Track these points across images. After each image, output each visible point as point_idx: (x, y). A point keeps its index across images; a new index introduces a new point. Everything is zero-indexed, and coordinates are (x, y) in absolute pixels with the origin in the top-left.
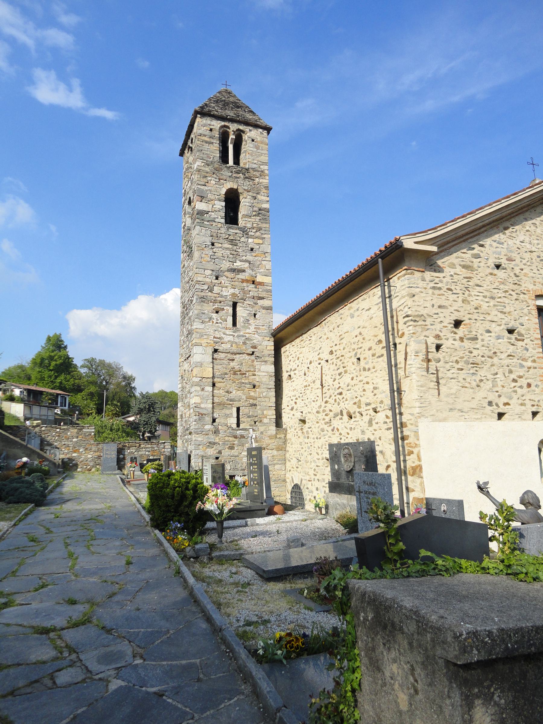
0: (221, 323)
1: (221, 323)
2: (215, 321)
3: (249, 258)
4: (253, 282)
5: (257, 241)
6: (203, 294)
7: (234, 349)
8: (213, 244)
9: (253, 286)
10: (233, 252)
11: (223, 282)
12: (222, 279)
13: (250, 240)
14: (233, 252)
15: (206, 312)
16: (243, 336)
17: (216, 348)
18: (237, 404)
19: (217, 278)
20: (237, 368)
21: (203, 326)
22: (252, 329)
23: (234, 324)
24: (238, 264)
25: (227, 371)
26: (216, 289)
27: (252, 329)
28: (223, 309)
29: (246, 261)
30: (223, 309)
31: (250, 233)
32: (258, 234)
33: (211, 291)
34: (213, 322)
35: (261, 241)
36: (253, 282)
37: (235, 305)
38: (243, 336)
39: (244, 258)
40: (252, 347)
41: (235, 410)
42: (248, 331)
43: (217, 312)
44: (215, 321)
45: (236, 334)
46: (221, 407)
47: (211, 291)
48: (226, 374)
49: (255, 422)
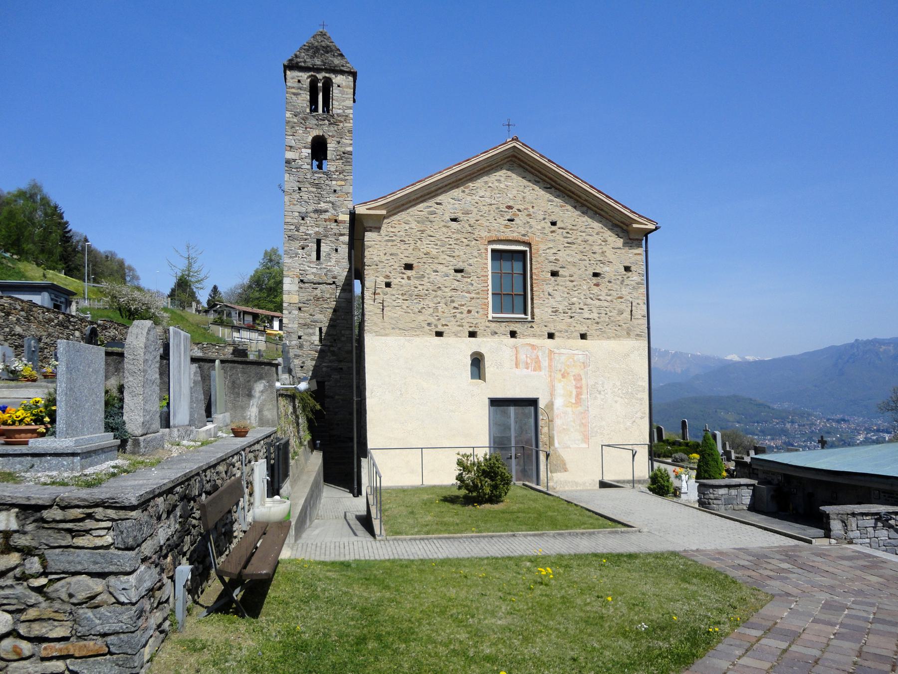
0: (305, 258)
1: (305, 258)
2: (300, 256)
3: (332, 199)
4: (336, 221)
5: (340, 183)
6: (290, 233)
7: (317, 279)
8: (300, 189)
9: (335, 224)
10: (317, 195)
11: (308, 222)
12: (308, 220)
13: (334, 182)
14: (317, 195)
15: (293, 248)
16: (325, 268)
17: (302, 278)
18: (319, 325)
19: (303, 219)
20: (319, 295)
21: (291, 260)
22: (333, 262)
23: (318, 258)
24: (323, 205)
25: (312, 298)
26: (302, 229)
27: (333, 262)
28: (308, 246)
29: (330, 202)
30: (308, 246)
31: (334, 176)
32: (341, 176)
33: (298, 230)
34: (299, 257)
35: (343, 183)
36: (336, 221)
37: (319, 242)
38: (325, 268)
39: (328, 199)
40: (333, 278)
41: (317, 329)
42: (329, 264)
43: (303, 248)
44: (300, 256)
45: (319, 267)
46: (306, 327)
47: (298, 230)
48: (310, 300)
49: (335, 340)
